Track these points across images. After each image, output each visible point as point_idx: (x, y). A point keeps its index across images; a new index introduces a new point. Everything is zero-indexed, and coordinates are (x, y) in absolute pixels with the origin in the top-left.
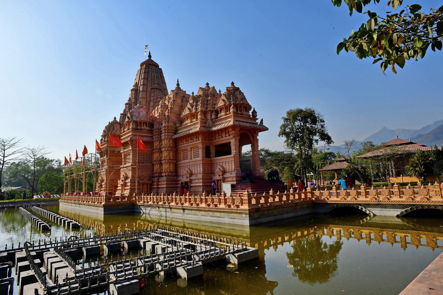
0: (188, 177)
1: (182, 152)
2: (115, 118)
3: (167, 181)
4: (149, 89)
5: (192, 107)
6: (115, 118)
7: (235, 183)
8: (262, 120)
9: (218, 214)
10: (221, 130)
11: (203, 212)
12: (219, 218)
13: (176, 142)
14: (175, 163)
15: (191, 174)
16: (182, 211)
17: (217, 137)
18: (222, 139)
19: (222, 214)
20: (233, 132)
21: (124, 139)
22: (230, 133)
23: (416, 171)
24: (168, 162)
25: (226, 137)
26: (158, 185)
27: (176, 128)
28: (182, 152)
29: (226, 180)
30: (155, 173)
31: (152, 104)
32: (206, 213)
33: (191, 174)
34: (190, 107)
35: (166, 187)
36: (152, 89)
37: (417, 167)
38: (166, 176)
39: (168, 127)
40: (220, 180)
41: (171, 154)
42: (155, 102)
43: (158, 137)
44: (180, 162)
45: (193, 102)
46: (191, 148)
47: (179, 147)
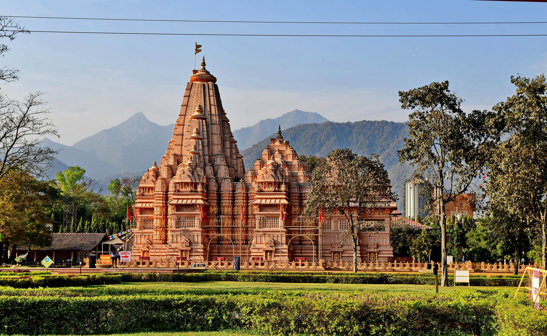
40: (375, 253)
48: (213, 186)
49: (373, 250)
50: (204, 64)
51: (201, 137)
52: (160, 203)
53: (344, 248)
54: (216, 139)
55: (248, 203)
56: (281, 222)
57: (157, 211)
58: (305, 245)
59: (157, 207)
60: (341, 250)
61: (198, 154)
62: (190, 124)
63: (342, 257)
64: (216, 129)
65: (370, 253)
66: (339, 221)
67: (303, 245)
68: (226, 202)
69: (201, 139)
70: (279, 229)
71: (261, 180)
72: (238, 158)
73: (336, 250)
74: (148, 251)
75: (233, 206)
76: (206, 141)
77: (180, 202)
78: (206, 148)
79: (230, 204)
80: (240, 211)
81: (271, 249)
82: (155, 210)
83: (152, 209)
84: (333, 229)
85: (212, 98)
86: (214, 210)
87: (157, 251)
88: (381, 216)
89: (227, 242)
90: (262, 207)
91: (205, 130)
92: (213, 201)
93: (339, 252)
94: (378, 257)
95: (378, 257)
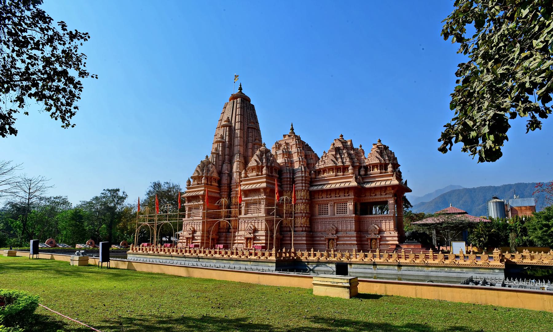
0: (332, 234)
1: (317, 206)
2: (207, 157)
3: (306, 237)
4: (246, 128)
5: (337, 159)
6: (207, 157)
7: (397, 243)
8: (406, 182)
9: (459, 270)
10: (376, 189)
11: (434, 269)
12: (459, 274)
13: (312, 195)
14: (311, 217)
15: (337, 231)
16: (396, 268)
17: (368, 194)
18: (376, 197)
19: (465, 270)
20: (392, 191)
21: (244, 185)
22: (388, 192)
23: (480, 241)
24: (305, 216)
25: (381, 195)
26: (226, 240)
27: (311, 179)
28: (317, 206)
29: (340, 239)
30: (285, 227)
31: (250, 145)
32: (439, 269)
33: (337, 231)
34: (334, 160)
35: (306, 244)
36: (248, 128)
37: (481, 237)
38: (302, 231)
39: (306, 177)
40: (376, 239)
41: (308, 207)
42: (254, 144)
43: (290, 188)
44: (315, 217)
45: (336, 154)
46: (334, 203)
47: (316, 200)
48: (225, 180)
49: (373, 236)
53: (340, 234)
56: (263, 207)
60: (335, 236)
63: (337, 244)
65: (371, 239)
66: (336, 205)
70: (260, 215)
73: (330, 236)
78: (227, 149)
81: (249, 236)
84: (329, 214)
85: (238, 110)
88: (383, 196)
90: (247, 193)
92: (224, 193)
93: (333, 239)
94: (380, 245)
95: (380, 245)
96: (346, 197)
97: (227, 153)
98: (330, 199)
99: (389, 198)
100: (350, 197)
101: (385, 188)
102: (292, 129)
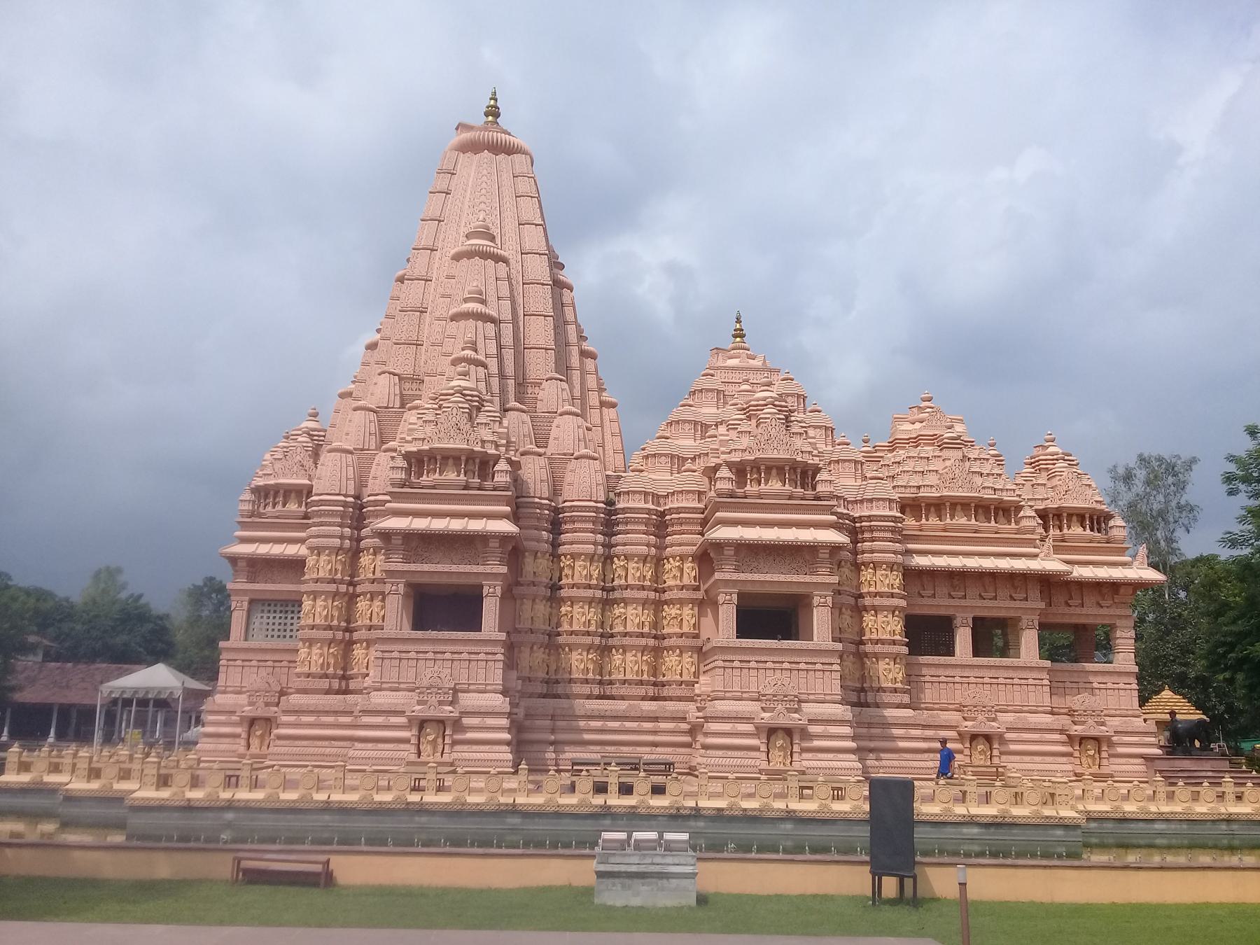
50: (493, 112)
51: (494, 314)
52: (332, 532)
54: (539, 332)
55: (661, 547)
57: (321, 567)
58: (877, 706)
59: (318, 550)
61: (485, 366)
62: (453, 272)
64: (540, 299)
67: (867, 705)
68: (581, 540)
69: (492, 320)
71: (735, 457)
72: (603, 404)
74: (268, 720)
75: (608, 559)
76: (507, 330)
77: (420, 524)
78: (509, 355)
79: (600, 550)
80: (633, 573)
82: (311, 561)
83: (295, 566)
86: (537, 567)
87: (305, 719)
89: (586, 689)
91: (505, 292)
96: (1018, 604)
97: (510, 370)
98: (963, 603)
99: (1120, 617)
100: (1029, 604)
101: (1114, 586)
102: (739, 334)
